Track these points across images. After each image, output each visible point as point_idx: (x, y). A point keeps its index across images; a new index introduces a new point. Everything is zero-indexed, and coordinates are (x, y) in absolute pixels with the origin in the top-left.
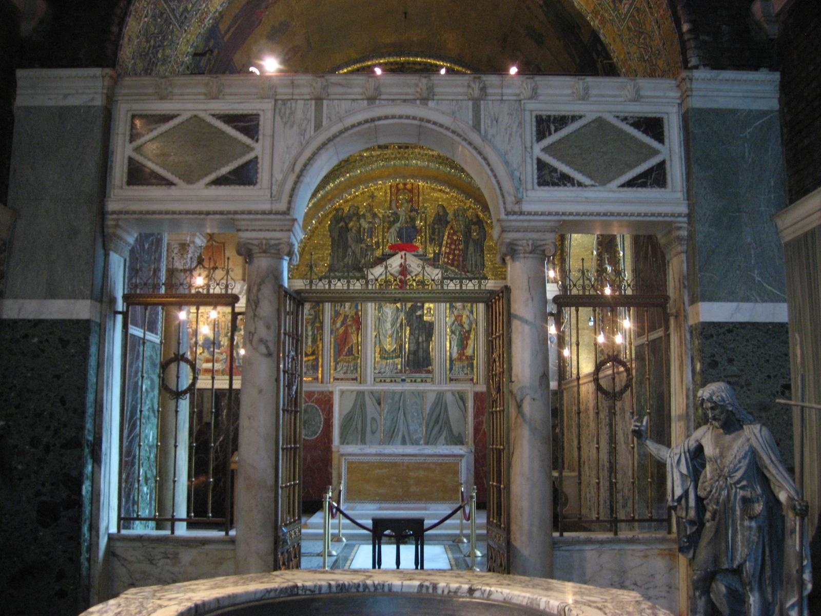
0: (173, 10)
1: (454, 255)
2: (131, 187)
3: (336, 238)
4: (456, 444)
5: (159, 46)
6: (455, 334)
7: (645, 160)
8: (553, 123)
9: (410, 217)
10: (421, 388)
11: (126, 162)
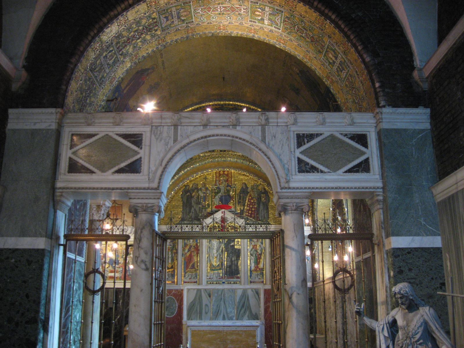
0: (96, 77)
1: (252, 211)
2: (70, 174)
3: (185, 201)
4: (254, 320)
5: (88, 96)
6: (253, 256)
7: (357, 158)
8: (306, 138)
9: (227, 190)
11: (68, 160)
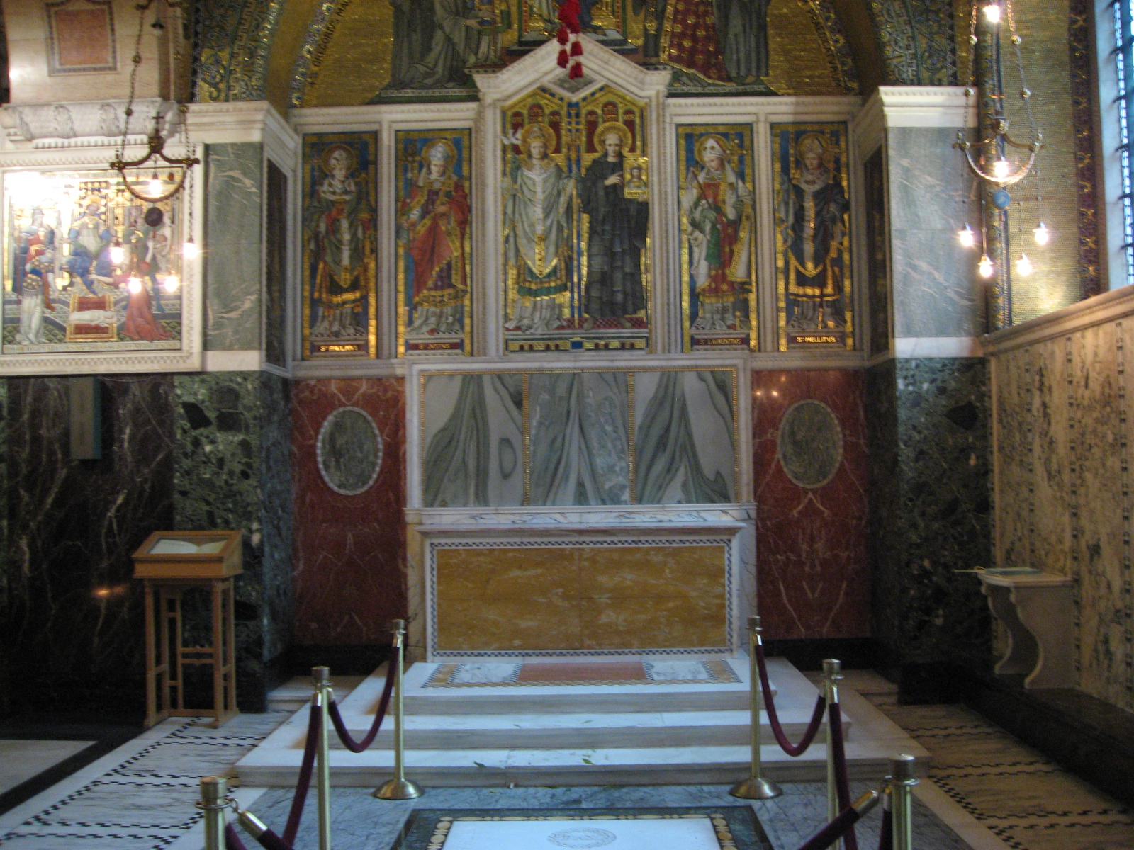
1: (694, 38)
4: (712, 501)
6: (702, 231)
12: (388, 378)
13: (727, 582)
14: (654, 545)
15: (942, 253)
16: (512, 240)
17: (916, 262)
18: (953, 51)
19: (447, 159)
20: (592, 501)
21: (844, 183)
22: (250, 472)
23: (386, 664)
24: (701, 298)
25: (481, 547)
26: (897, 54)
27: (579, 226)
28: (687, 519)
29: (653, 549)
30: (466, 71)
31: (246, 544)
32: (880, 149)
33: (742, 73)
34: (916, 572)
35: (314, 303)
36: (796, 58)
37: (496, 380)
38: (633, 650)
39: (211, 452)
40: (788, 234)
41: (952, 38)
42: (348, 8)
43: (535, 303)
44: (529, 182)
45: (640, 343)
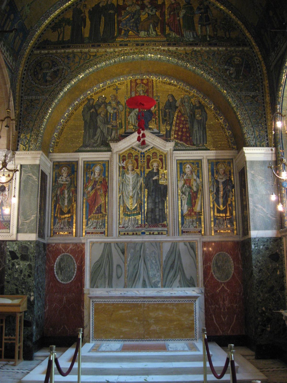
1: (182, 132)
3: (88, 121)
4: (189, 287)
6: (185, 195)
10: (158, 240)
12: (79, 243)
13: (195, 315)
14: (169, 302)
15: (265, 202)
16: (122, 197)
17: (257, 205)
18: (267, 136)
19: (101, 170)
20: (148, 287)
21: (232, 179)
22: (31, 275)
23: (76, 343)
24: (185, 217)
25: (110, 302)
26: (249, 137)
27: (144, 193)
28: (181, 293)
29: (169, 303)
30: (107, 142)
31: (29, 300)
32: (244, 167)
33: (198, 143)
34: (260, 312)
35: (55, 218)
36: (216, 138)
37: (116, 244)
38: (162, 339)
39: (18, 268)
40: (214, 196)
41: (266, 132)
42: (69, 121)
43: (129, 219)
44: (127, 178)
45: (165, 232)
